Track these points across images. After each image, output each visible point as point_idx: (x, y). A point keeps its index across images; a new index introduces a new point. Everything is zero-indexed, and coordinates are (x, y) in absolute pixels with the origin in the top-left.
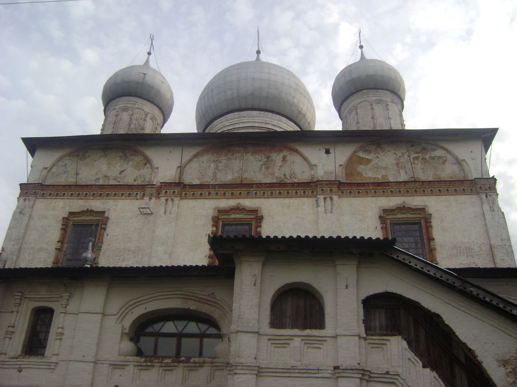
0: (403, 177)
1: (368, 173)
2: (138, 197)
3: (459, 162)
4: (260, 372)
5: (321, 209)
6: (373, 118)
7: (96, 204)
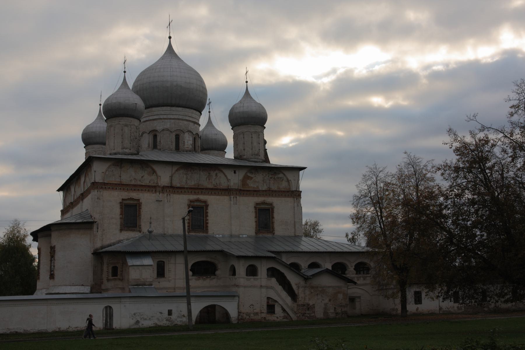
0: (265, 188)
1: (252, 185)
2: (153, 192)
3: (288, 181)
4: (245, 287)
5: (232, 202)
6: (252, 143)
7: (134, 195)
